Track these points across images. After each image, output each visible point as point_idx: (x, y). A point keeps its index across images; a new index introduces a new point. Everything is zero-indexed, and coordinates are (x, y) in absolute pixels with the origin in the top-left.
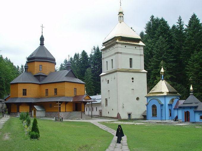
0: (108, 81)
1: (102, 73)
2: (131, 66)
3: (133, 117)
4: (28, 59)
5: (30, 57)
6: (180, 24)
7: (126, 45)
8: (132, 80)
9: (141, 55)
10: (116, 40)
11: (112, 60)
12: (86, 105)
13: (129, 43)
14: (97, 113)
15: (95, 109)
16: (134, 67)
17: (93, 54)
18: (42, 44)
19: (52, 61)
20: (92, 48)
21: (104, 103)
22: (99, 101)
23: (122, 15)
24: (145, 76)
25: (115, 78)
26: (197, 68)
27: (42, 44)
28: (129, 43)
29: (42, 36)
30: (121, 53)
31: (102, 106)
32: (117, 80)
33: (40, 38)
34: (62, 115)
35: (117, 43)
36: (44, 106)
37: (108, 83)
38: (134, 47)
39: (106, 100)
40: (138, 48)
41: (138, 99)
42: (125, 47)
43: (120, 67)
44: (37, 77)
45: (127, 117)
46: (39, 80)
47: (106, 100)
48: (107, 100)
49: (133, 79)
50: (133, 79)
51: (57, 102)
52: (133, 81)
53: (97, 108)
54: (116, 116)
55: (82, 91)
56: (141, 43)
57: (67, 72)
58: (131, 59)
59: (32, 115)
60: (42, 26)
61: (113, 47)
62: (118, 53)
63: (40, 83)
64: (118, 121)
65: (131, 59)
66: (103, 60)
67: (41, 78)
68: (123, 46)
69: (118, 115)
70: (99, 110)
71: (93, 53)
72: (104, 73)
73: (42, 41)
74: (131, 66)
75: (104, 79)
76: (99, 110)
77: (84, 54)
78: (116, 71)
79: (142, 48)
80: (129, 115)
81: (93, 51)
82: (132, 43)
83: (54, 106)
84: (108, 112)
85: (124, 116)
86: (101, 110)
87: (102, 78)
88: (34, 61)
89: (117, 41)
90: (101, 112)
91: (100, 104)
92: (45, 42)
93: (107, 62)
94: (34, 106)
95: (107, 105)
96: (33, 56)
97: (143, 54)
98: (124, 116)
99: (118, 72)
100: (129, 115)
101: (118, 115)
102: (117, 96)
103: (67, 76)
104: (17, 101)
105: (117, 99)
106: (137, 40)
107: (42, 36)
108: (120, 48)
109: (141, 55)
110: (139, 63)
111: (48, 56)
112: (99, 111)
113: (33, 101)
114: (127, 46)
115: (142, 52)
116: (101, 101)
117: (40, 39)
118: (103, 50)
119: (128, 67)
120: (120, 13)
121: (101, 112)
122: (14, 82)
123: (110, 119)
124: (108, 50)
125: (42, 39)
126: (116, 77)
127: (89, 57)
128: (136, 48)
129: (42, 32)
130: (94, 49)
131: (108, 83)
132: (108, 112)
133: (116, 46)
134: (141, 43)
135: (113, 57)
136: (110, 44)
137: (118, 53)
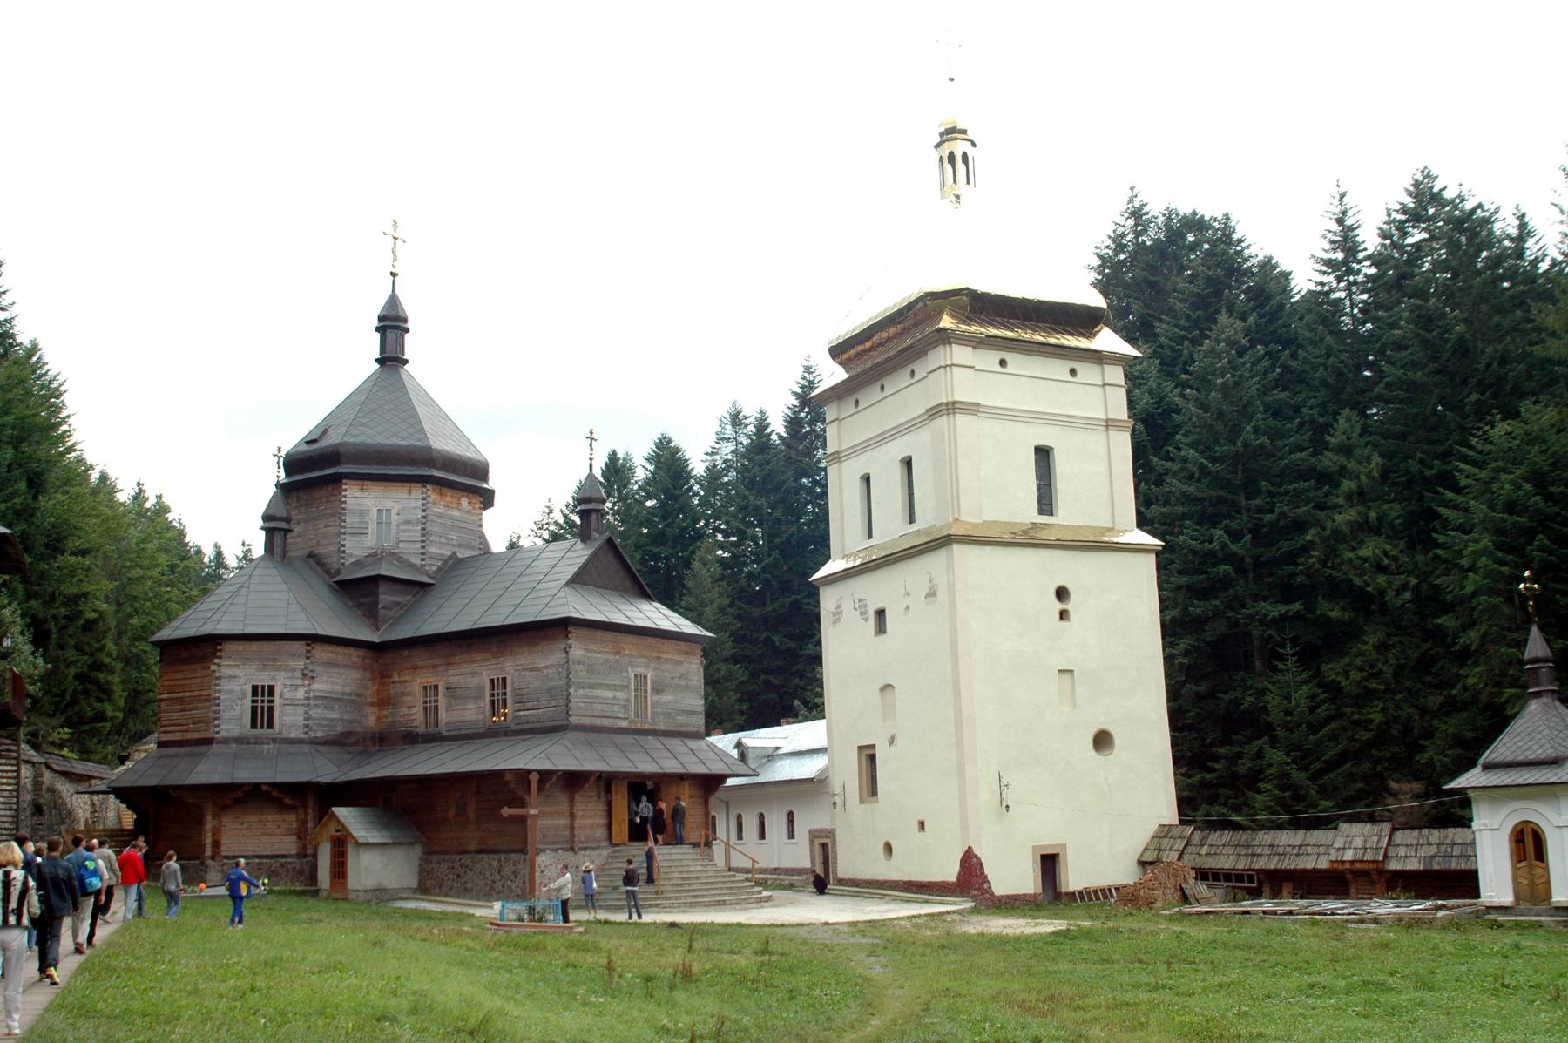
0: (881, 614)
1: (829, 558)
2: (1046, 502)
3: (1074, 878)
4: (293, 463)
5: (305, 448)
6: (1340, 221)
7: (1007, 356)
8: (1059, 606)
9: (1109, 425)
10: (937, 316)
11: (908, 463)
12: (718, 794)
13: (1026, 335)
14: (800, 855)
15: (777, 825)
16: (1071, 513)
17: (727, 449)
18: (391, 359)
19: (466, 480)
20: (724, 411)
21: (848, 776)
22: (807, 769)
23: (966, 147)
24: (1147, 567)
25: (932, 594)
26: (1511, 507)
27: (391, 359)
28: (1026, 335)
29: (393, 301)
30: (973, 409)
31: (837, 799)
32: (952, 603)
33: (381, 319)
34: (558, 877)
35: (945, 337)
36: (412, 807)
37: (881, 628)
38: (1059, 368)
39: (869, 757)
40: (1088, 372)
41: (1102, 741)
42: (1003, 363)
43: (978, 511)
44: (359, 590)
45: (1026, 881)
46: (371, 615)
47: (869, 757)
48: (872, 758)
49: (1062, 594)
50: (1062, 594)
51: (523, 775)
52: (1063, 615)
53: (791, 815)
54: (950, 872)
55: (684, 688)
56: (1107, 340)
57: (577, 554)
58: (1043, 454)
59: (313, 878)
60: (390, 230)
61: (914, 366)
62: (950, 408)
63: (375, 638)
64: (973, 911)
65: (1043, 454)
66: (832, 473)
67: (386, 597)
68: (989, 359)
69: (971, 864)
70: (814, 834)
71: (730, 447)
72: (845, 557)
73: (391, 335)
74: (1046, 502)
75: (847, 607)
76: (814, 834)
77: (668, 459)
78: (944, 541)
79: (1116, 375)
80: (1049, 863)
81: (729, 432)
82: (1052, 341)
83: (506, 811)
84: (888, 848)
85: (1012, 874)
86: (831, 833)
87: (828, 601)
88: (337, 480)
89: (946, 322)
90: (825, 847)
91: (812, 788)
92: (412, 346)
93: (867, 479)
94: (334, 809)
95: (871, 788)
96: (323, 443)
97: (1122, 412)
98: (1012, 874)
99: (956, 547)
100: (1049, 863)
101: (971, 864)
102: (958, 723)
103: (579, 579)
104: (208, 771)
105: (959, 742)
106: (1081, 320)
107: (393, 301)
108: (967, 372)
109: (1109, 425)
110: (1101, 480)
111: (440, 443)
112: (812, 843)
113: (327, 770)
114: (1017, 362)
115: (1118, 406)
116: (820, 762)
117: (376, 323)
118: (838, 393)
119: (1027, 512)
120: (951, 133)
121: (824, 846)
122: (179, 634)
123: (927, 902)
124: (870, 395)
125: (392, 324)
126: (941, 582)
127: (698, 467)
128: (1073, 372)
129: (393, 275)
130: (736, 419)
131: (881, 628)
132: (888, 848)
133: (939, 356)
134: (1107, 340)
135: (916, 444)
136: (888, 348)
137: (950, 408)
